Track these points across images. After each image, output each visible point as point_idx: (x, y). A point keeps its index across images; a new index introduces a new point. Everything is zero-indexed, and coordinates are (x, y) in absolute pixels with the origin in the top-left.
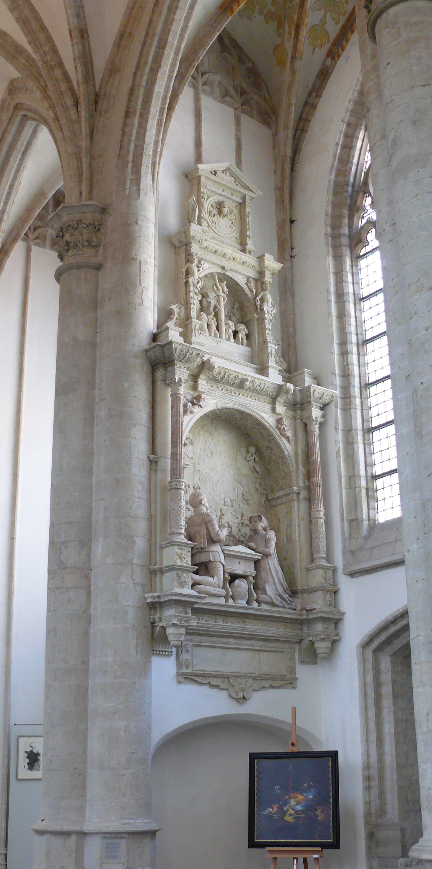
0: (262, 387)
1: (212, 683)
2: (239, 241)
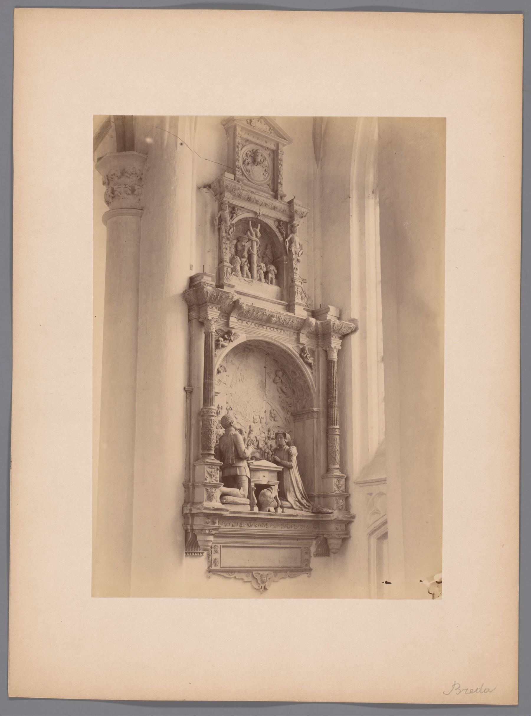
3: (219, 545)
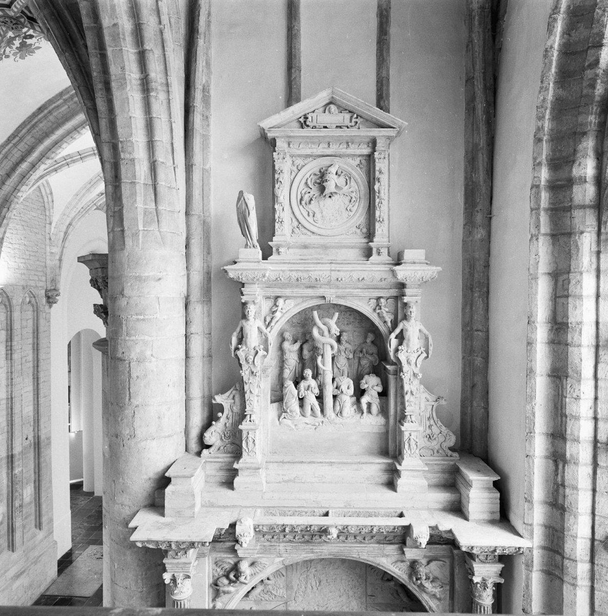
2: (365, 230)
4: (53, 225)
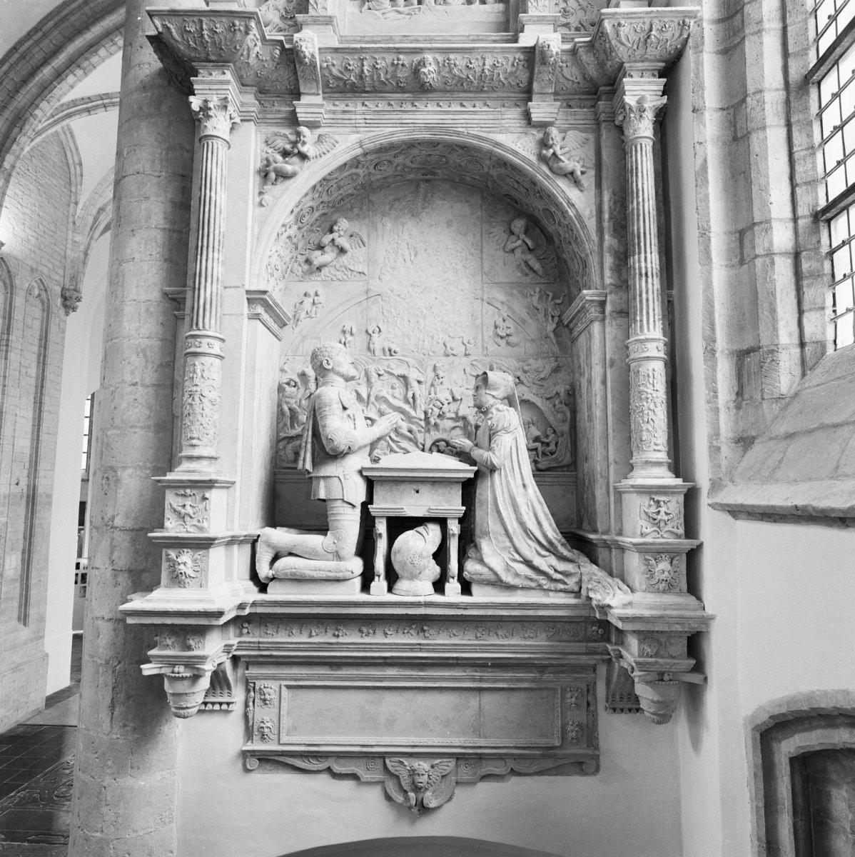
0: (478, 70)
1: (337, 768)
3: (274, 685)
4: (80, 206)
